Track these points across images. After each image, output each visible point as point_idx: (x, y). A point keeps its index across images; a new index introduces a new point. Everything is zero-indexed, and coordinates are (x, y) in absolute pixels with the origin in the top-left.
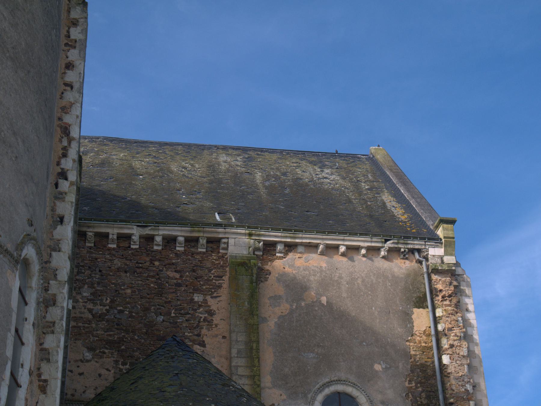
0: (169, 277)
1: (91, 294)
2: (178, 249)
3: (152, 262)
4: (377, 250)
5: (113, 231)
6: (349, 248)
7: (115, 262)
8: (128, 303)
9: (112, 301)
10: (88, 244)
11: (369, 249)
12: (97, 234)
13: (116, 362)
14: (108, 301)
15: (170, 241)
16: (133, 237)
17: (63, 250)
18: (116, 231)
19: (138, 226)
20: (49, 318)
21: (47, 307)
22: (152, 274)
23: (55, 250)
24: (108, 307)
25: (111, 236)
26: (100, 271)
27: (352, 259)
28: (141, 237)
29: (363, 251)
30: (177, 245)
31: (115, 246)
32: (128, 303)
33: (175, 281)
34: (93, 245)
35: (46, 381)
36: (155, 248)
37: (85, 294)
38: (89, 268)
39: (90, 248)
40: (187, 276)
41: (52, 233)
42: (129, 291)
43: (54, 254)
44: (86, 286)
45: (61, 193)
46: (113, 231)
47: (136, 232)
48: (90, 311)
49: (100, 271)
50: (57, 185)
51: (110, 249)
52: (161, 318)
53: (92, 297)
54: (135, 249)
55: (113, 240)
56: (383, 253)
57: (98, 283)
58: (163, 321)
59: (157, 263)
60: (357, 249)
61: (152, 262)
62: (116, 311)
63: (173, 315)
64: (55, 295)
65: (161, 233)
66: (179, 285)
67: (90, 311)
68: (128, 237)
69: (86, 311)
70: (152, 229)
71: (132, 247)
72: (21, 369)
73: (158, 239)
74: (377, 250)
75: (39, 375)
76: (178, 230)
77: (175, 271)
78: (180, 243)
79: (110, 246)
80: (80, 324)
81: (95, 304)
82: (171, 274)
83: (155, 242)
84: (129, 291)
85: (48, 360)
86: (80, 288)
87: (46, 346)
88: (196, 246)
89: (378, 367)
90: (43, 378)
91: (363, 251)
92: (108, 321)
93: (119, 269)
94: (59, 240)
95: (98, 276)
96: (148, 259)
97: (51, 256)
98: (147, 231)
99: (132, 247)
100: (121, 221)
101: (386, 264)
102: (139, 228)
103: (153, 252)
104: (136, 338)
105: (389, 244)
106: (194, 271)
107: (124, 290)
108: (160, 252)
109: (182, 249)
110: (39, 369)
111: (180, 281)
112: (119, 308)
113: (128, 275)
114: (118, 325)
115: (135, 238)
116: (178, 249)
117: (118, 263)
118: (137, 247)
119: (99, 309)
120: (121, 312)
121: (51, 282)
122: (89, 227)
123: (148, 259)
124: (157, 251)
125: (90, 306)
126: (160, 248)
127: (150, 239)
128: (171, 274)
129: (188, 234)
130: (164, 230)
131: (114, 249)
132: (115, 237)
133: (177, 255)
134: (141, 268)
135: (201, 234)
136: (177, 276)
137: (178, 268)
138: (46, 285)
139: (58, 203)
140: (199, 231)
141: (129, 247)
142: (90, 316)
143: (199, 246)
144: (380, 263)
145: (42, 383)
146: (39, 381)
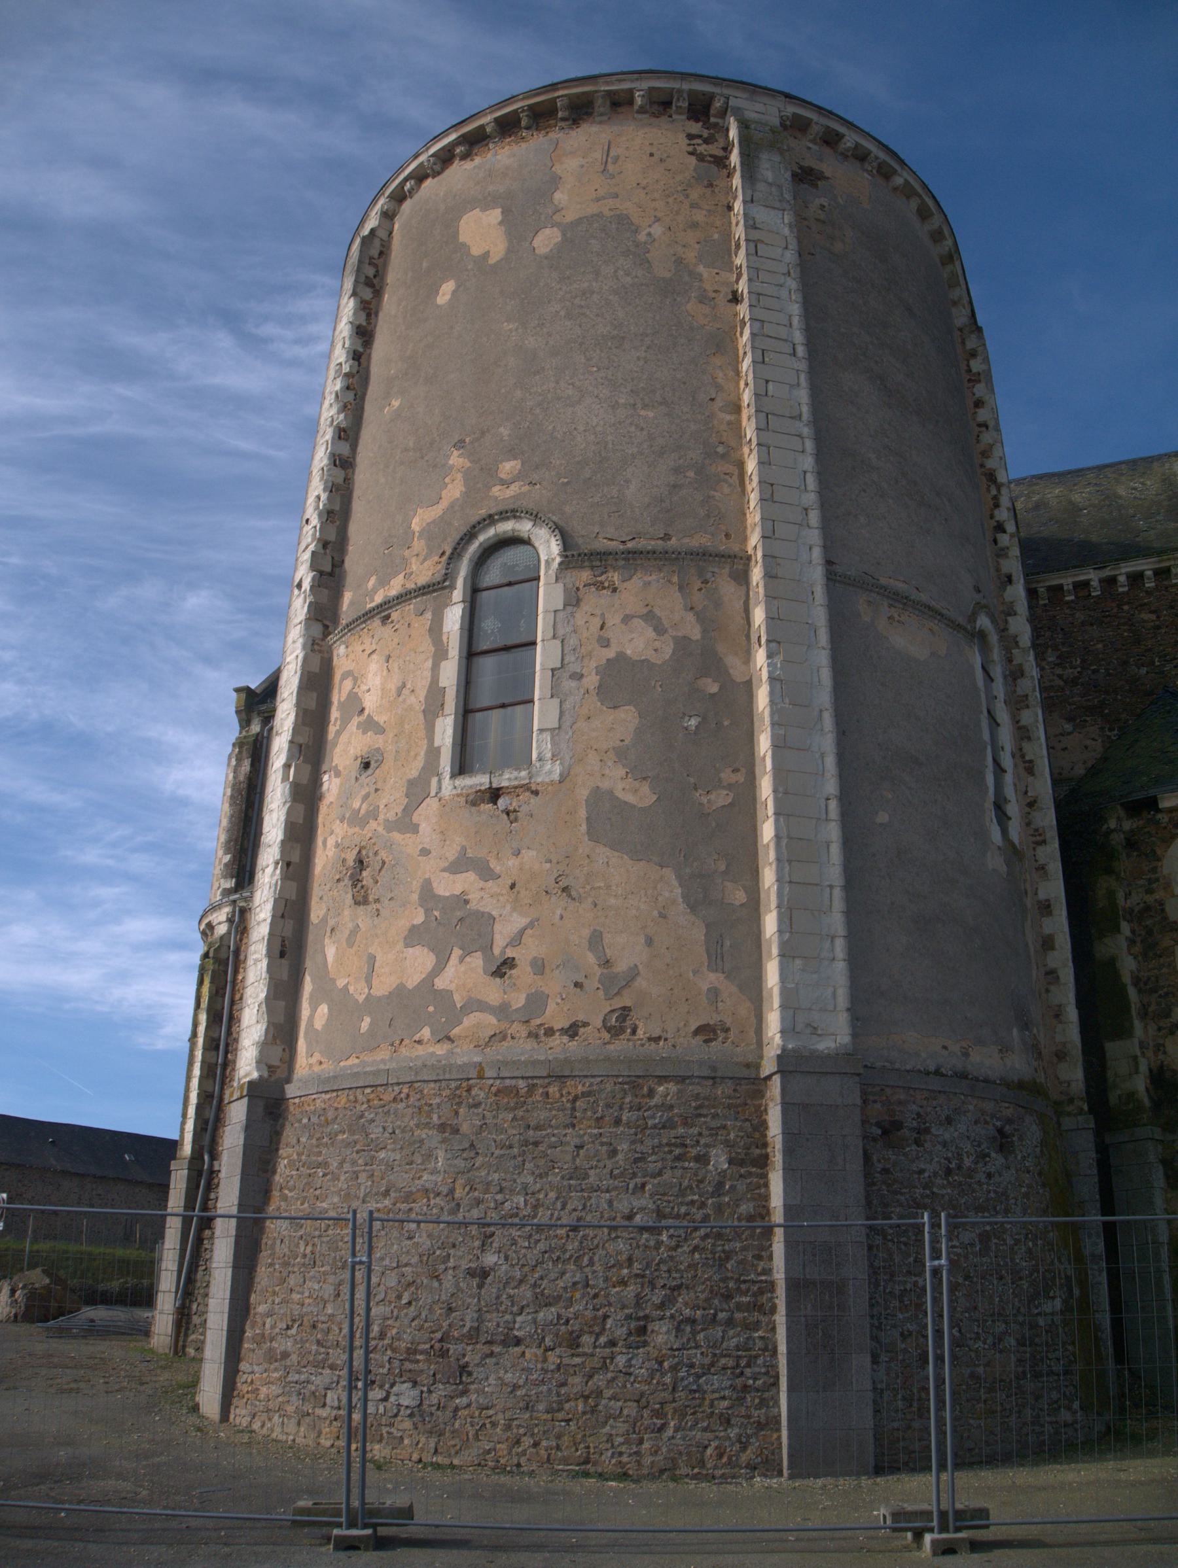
0: (1144, 621)
1: (1057, 658)
2: (1147, 585)
3: (1119, 607)
5: (1067, 581)
7: (1078, 615)
8: (1103, 660)
9: (1083, 661)
10: (1042, 602)
12: (1050, 589)
13: (1102, 729)
14: (1078, 662)
15: (1136, 578)
16: (1092, 583)
17: (1019, 612)
18: (1070, 580)
19: (1095, 569)
20: (1019, 692)
21: (1015, 679)
22: (1122, 621)
23: (1009, 615)
24: (1079, 669)
25: (1065, 588)
26: (1062, 629)
28: (1101, 581)
30: (1146, 581)
31: (1072, 598)
32: (1103, 660)
33: (1152, 624)
34: (1047, 601)
35: (1031, 761)
36: (1121, 590)
37: (1050, 659)
38: (1049, 628)
39: (1045, 605)
40: (1165, 615)
41: (1002, 595)
42: (1100, 646)
43: (1010, 619)
44: (1050, 650)
45: (1002, 549)
46: (1067, 581)
47: (1093, 576)
48: (1060, 677)
49: (1062, 629)
50: (995, 541)
51: (1068, 602)
52: (1144, 670)
53: (1059, 661)
54: (1097, 596)
55: (1069, 591)
57: (1063, 644)
58: (1147, 672)
59: (1126, 608)
61: (1119, 607)
62: (1090, 672)
63: (1157, 664)
64: (1020, 665)
65: (1123, 571)
66: (1158, 627)
67: (1060, 677)
68: (1086, 584)
69: (1055, 678)
70: (1112, 569)
71: (1093, 594)
72: (1002, 753)
73: (1122, 579)
75: (1023, 756)
76: (1142, 564)
77: (1150, 612)
78: (1149, 578)
79: (1067, 598)
80: (1052, 694)
81: (1064, 668)
82: (1145, 616)
83: (1119, 584)
84: (1100, 646)
85: (1029, 739)
86: (1043, 653)
87: (1023, 723)
88: (1168, 578)
90: (1027, 758)
92: (1082, 684)
93: (1083, 624)
94: (1012, 603)
95: (1060, 636)
96: (1114, 605)
97: (1006, 622)
98: (1107, 572)
99: (1093, 594)
100: (1075, 567)
102: (1097, 571)
103: (1118, 594)
104: (1119, 697)
106: (1172, 607)
107: (1094, 645)
108: (1127, 593)
109: (1153, 584)
110: (1021, 749)
111: (1157, 623)
112: (1092, 668)
113: (1095, 627)
114: (1095, 687)
115: (1095, 583)
116: (1147, 585)
117: (1080, 616)
118: (1099, 593)
119: (1070, 673)
120: (1094, 671)
121: (1013, 651)
122: (1038, 582)
123: (1114, 605)
124: (1123, 593)
125: (1059, 671)
126: (1126, 589)
127: (1112, 580)
128: (1145, 616)
129: (1157, 566)
130: (1126, 567)
131: (1072, 601)
132: (1071, 587)
133: (1149, 593)
134: (1109, 616)
135: (1172, 563)
136: (1153, 617)
137: (1153, 608)
138: (1009, 655)
139: (1001, 561)
140: (1169, 559)
141: (1090, 595)
142: (1062, 683)
143: (1172, 576)
145: (1027, 765)
146: (1025, 762)
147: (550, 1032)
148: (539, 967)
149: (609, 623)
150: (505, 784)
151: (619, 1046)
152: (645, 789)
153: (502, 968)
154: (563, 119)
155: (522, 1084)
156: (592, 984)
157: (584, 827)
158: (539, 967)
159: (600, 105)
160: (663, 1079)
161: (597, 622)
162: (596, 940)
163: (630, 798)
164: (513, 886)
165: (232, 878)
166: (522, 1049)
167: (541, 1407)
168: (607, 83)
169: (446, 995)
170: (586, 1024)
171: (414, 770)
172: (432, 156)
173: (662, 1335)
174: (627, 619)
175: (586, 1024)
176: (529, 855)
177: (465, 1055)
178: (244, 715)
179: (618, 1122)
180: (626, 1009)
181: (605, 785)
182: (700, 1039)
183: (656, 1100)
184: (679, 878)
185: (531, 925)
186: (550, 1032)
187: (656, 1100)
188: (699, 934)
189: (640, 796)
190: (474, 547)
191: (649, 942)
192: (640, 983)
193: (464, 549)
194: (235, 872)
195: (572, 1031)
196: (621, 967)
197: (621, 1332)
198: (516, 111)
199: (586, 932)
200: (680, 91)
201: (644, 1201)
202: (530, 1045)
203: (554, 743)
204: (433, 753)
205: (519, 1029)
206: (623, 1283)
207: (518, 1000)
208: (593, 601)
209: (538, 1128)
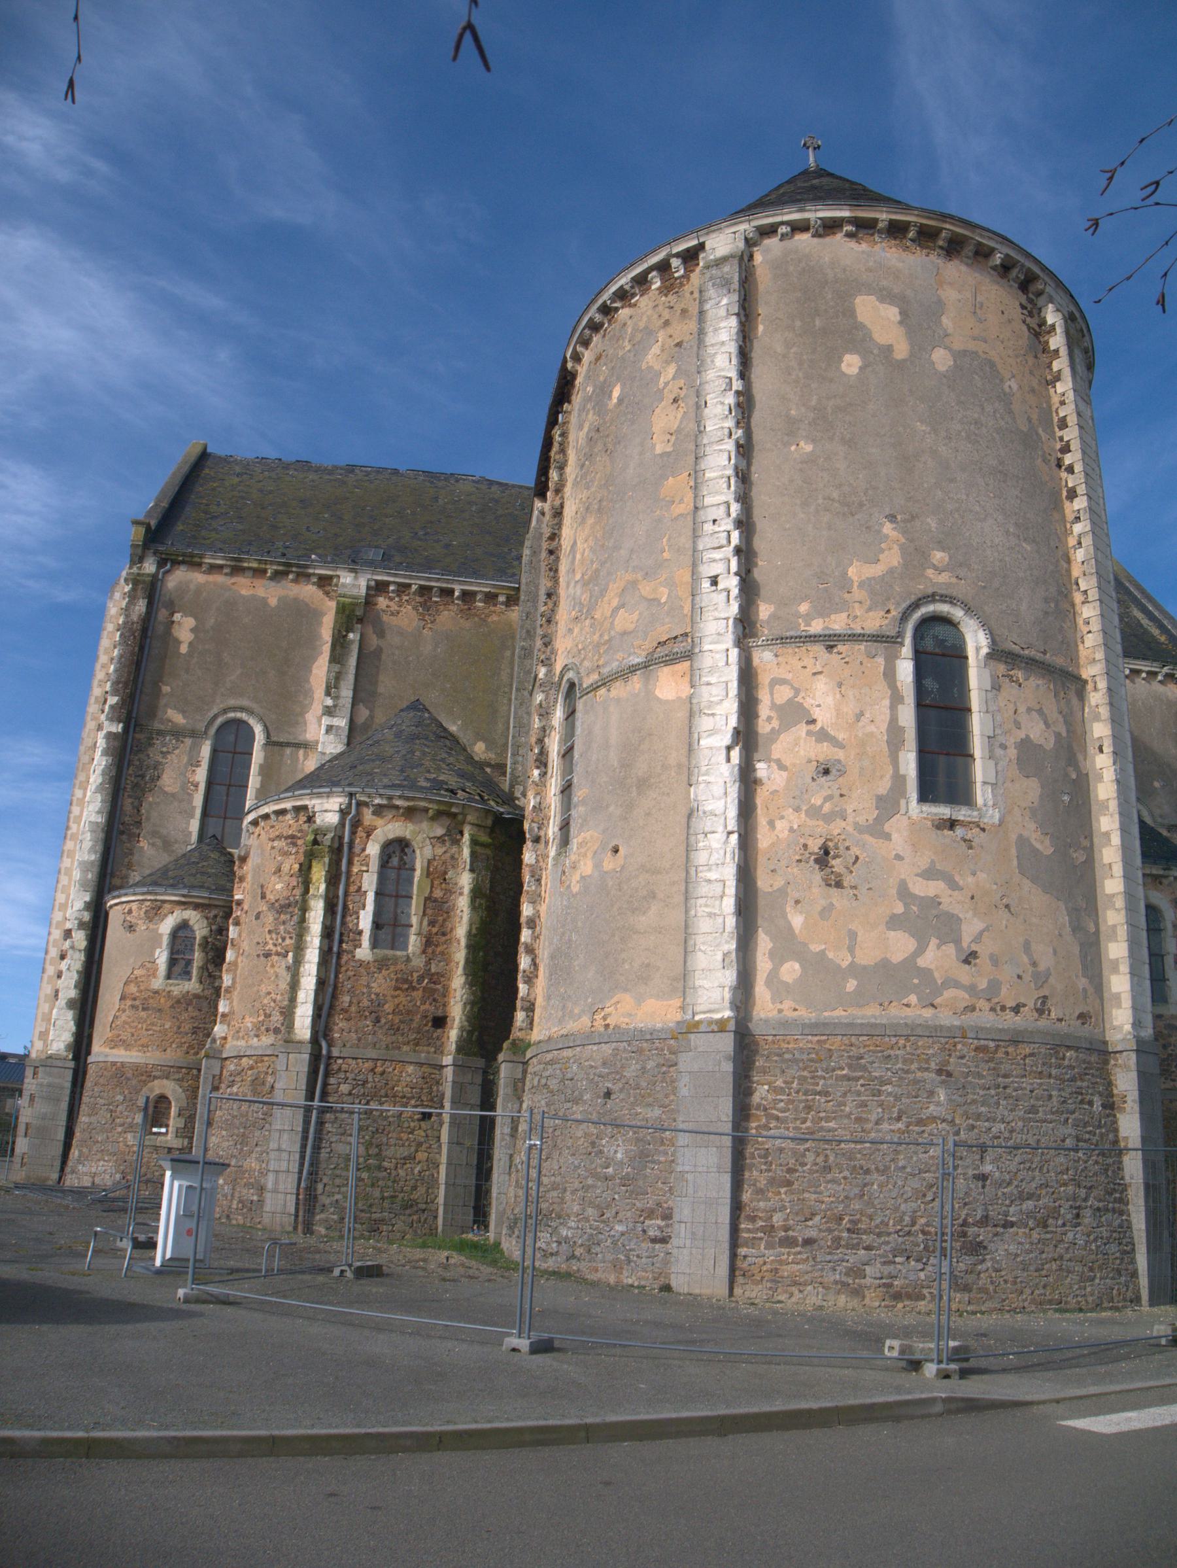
4: (1155, 674)
6: (1132, 670)
11: (1149, 673)
27: (1133, 682)
29: (1144, 675)
56: (1160, 678)
60: (1138, 672)
74: (1155, 674)
89: (1156, 784)
91: (1144, 675)
101: (1161, 689)
105: (1166, 670)
144: (1156, 687)
147: (1003, 1008)
148: (995, 961)
149: (1019, 711)
150: (961, 818)
151: (1043, 1023)
152: (1047, 842)
153: (970, 958)
154: (941, 248)
155: (992, 1044)
156: (1027, 977)
157: (1015, 862)
158: (995, 961)
159: (969, 250)
160: (1069, 1048)
161: (1011, 707)
162: (1027, 947)
163: (1038, 846)
164: (972, 898)
165: (120, 722)
166: (985, 1018)
167: (1032, 1268)
168: (981, 236)
169: (926, 974)
170: (1024, 1005)
171: (884, 786)
172: (820, 219)
173: (1087, 1219)
174: (1029, 710)
175: (1024, 1005)
176: (982, 876)
177: (946, 1018)
178: (139, 551)
179: (1050, 1076)
180: (1045, 997)
181: (1026, 834)
182: (1080, 1021)
183: (1066, 1062)
184: (1067, 908)
185: (986, 929)
186: (1003, 1008)
187: (1066, 1062)
188: (1076, 950)
189: (1045, 847)
190: (917, 615)
191: (1055, 953)
192: (1052, 980)
193: (910, 615)
194: (123, 717)
195: (1016, 1009)
196: (1042, 967)
197: (1069, 1216)
198: (910, 222)
199: (1021, 940)
200: (1023, 266)
201: (1069, 1130)
202: (992, 1016)
203: (994, 796)
204: (899, 780)
205: (982, 1004)
206: (1065, 1184)
207: (983, 984)
208: (1009, 690)
209: (1005, 1076)
